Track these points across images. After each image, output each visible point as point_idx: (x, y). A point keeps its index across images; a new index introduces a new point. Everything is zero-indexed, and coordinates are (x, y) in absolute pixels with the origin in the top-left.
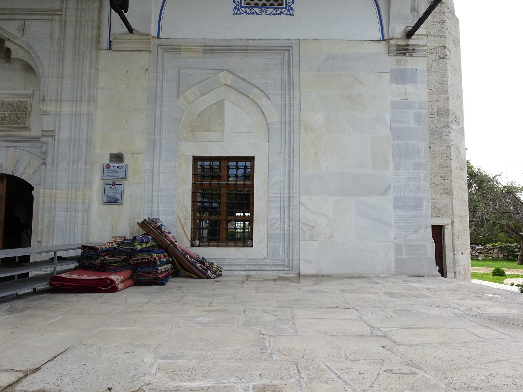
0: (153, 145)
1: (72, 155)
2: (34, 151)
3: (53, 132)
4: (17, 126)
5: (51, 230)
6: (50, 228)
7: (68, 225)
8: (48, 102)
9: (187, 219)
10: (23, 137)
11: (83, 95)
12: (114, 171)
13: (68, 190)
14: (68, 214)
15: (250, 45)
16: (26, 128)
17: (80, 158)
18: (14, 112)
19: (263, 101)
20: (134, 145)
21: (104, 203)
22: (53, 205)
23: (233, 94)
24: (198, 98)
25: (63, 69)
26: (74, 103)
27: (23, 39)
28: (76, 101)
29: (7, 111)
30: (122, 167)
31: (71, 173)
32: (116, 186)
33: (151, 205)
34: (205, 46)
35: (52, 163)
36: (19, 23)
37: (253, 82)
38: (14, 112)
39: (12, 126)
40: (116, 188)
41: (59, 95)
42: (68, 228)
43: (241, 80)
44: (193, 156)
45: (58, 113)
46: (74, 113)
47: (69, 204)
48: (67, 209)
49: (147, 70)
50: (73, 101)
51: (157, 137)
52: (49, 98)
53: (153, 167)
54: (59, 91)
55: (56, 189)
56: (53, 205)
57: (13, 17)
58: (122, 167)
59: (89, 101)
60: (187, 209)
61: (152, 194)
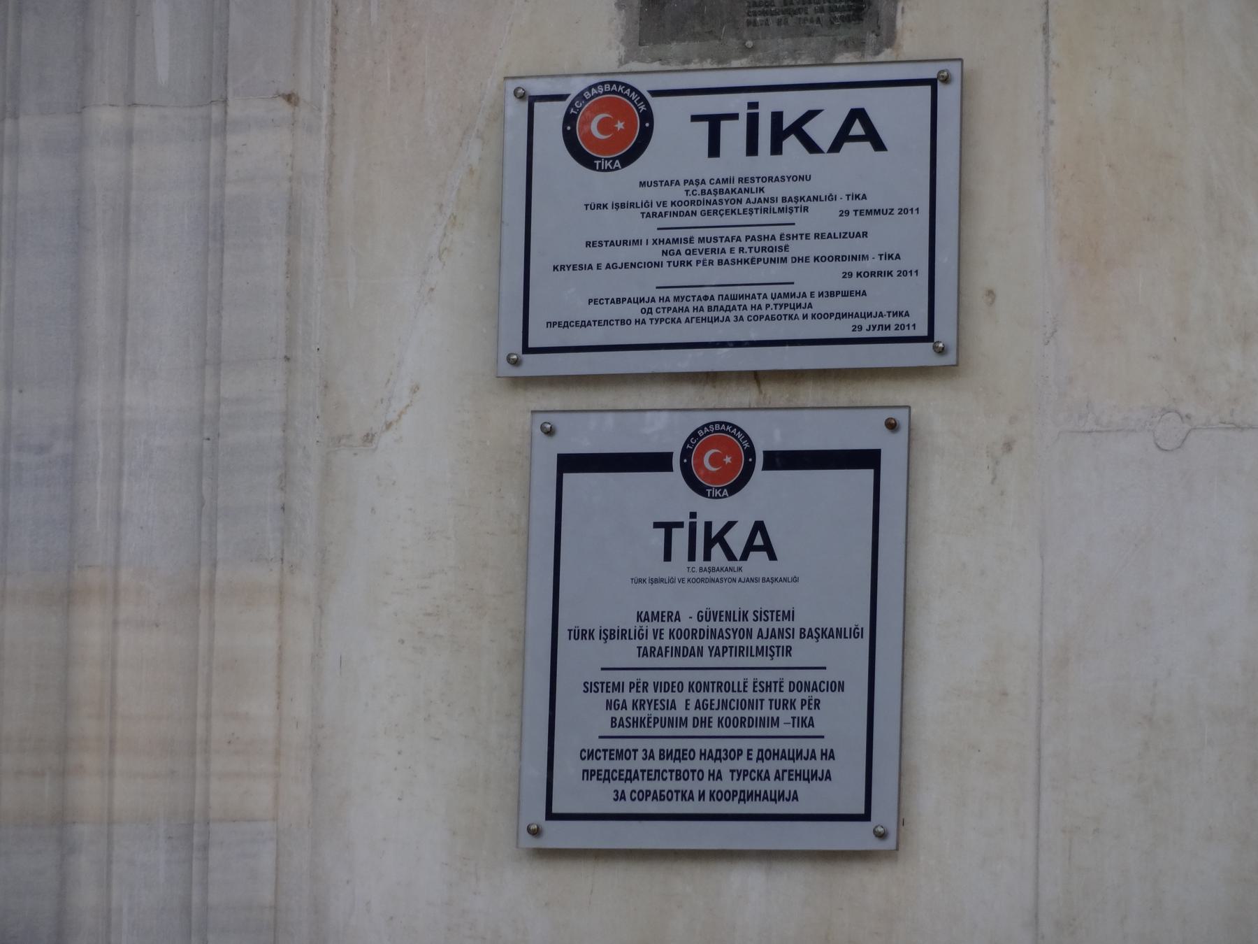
21: (552, 832)
30: (860, 129)
32: (767, 494)
40: (761, 540)
58: (860, 129)
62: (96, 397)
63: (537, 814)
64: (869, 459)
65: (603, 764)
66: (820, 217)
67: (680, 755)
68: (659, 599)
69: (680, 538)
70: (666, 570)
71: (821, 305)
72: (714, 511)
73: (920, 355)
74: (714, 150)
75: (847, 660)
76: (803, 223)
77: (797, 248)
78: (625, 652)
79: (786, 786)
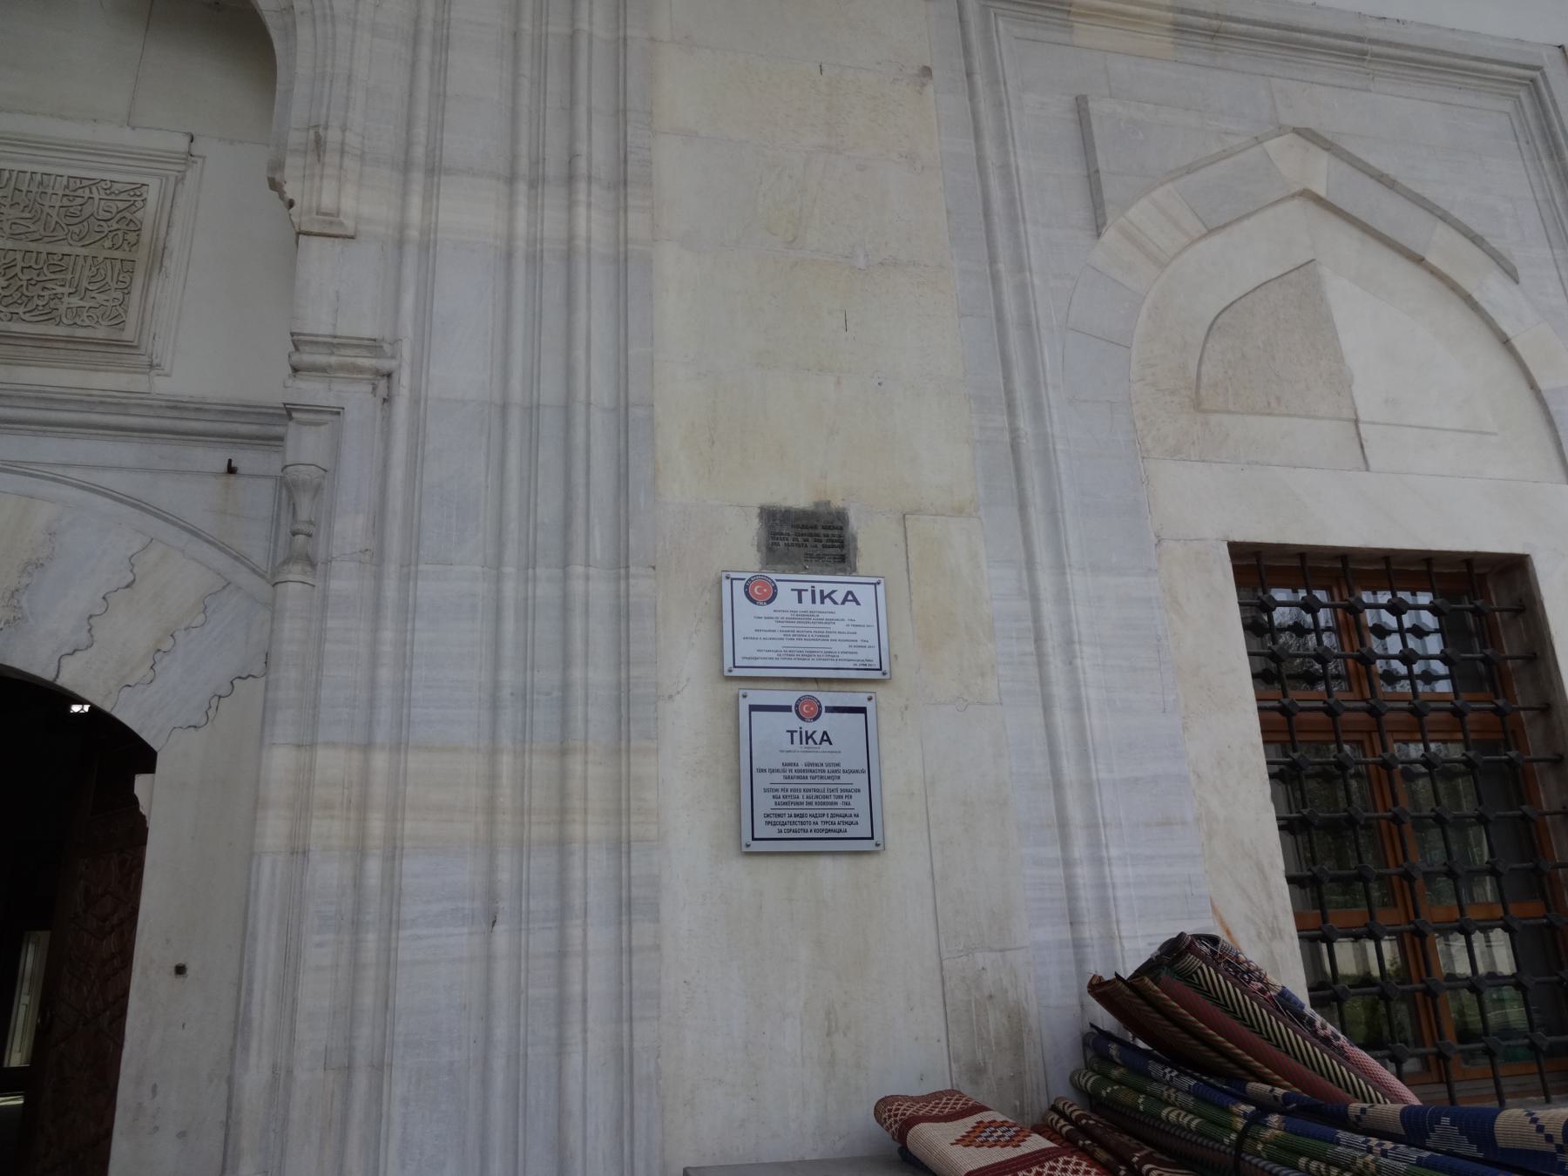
0: (1016, 468)
1: (513, 509)
3: (373, 346)
4: (61, 331)
5: (362, 1081)
6: (349, 1068)
7: (501, 1031)
9: (1276, 933)
10: (88, 401)
11: (582, 147)
12: (805, 617)
13: (494, 752)
14: (502, 938)
15: (1375, 35)
17: (579, 521)
18: (43, 248)
19: (1492, 289)
20: (904, 455)
22: (374, 867)
23: (1343, 243)
24: (1194, 242)
26: (522, 187)
31: (509, 626)
32: (827, 722)
33: (1054, 852)
34: (1183, 11)
35: (376, 556)
37: (1429, 193)
38: (43, 248)
40: (826, 737)
41: (421, 132)
42: (499, 1063)
43: (1371, 182)
44: (1239, 552)
45: (413, 234)
46: (521, 245)
47: (505, 860)
48: (491, 896)
49: (927, 71)
50: (511, 179)
51: (1025, 424)
52: (352, 139)
53: (1035, 598)
54: (422, 111)
55: (399, 747)
56: (374, 867)
58: (850, 597)
59: (621, 183)
60: (1261, 870)
61: (1056, 772)
62: (577, 674)
63: (747, 837)
64: (862, 710)
65: (773, 819)
66: (839, 626)
67: (802, 816)
68: (790, 758)
69: (796, 736)
70: (791, 747)
71: (842, 656)
72: (809, 727)
73: (877, 675)
74: (800, 601)
75: (860, 781)
76: (833, 627)
77: (832, 636)
78: (778, 777)
79: (842, 827)
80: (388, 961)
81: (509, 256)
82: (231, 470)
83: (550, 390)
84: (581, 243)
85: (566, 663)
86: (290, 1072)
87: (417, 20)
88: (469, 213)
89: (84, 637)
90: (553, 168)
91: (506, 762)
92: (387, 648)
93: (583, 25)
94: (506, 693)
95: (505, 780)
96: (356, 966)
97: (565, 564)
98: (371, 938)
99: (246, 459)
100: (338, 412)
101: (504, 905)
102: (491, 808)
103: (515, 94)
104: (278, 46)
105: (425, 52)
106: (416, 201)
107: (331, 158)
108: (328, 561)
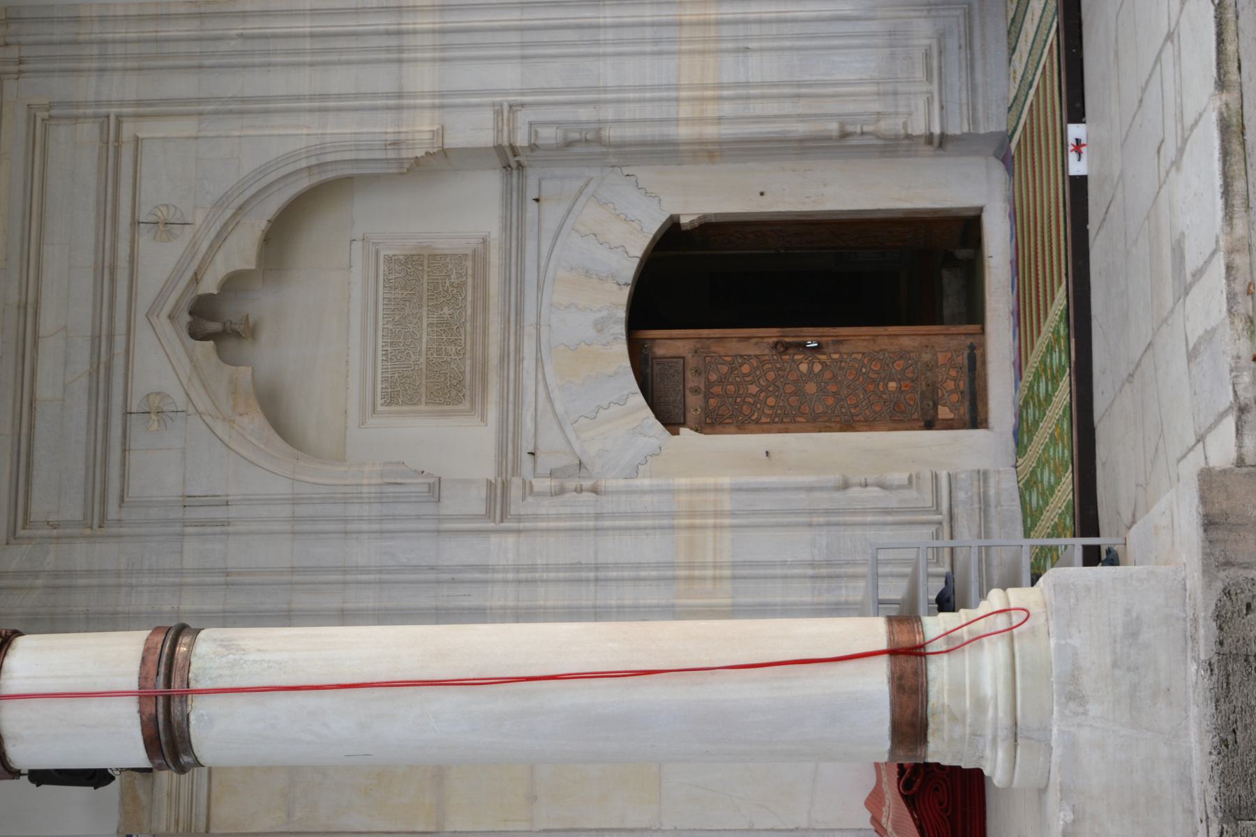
2: (550, 224)
3: (499, 113)
4: (470, 281)
6: (799, 96)
7: (788, 43)
8: (404, 129)
10: (507, 266)
11: (382, 27)
13: (680, 52)
14: (751, 45)
16: (479, 257)
22: (725, 93)
25: (299, 98)
26: (405, 56)
27: (199, 221)
28: (401, 49)
29: (420, 319)
36: (146, 242)
39: (469, 298)
41: (379, 102)
45: (437, 101)
46: (437, 55)
47: (724, 46)
48: (737, 50)
50: (400, 61)
54: (367, 103)
55: (678, 87)
56: (725, 93)
57: (123, 263)
62: (648, 19)
80: (762, 85)
81: (443, 60)
82: (537, 200)
83: (514, 37)
84: (437, 26)
85: (643, 25)
86: (799, 116)
87: (311, 110)
88: (423, 78)
89: (620, 249)
90: (393, 42)
91: (685, 47)
92: (637, 95)
93: (308, 30)
94: (656, 49)
95: (692, 47)
96: (763, 97)
97: (598, 27)
98: (752, 92)
99: (532, 193)
100: (531, 124)
101: (741, 45)
102: (703, 52)
103: (349, 63)
104: (330, 175)
105: (332, 104)
106: (419, 101)
107: (403, 137)
108: (599, 122)
